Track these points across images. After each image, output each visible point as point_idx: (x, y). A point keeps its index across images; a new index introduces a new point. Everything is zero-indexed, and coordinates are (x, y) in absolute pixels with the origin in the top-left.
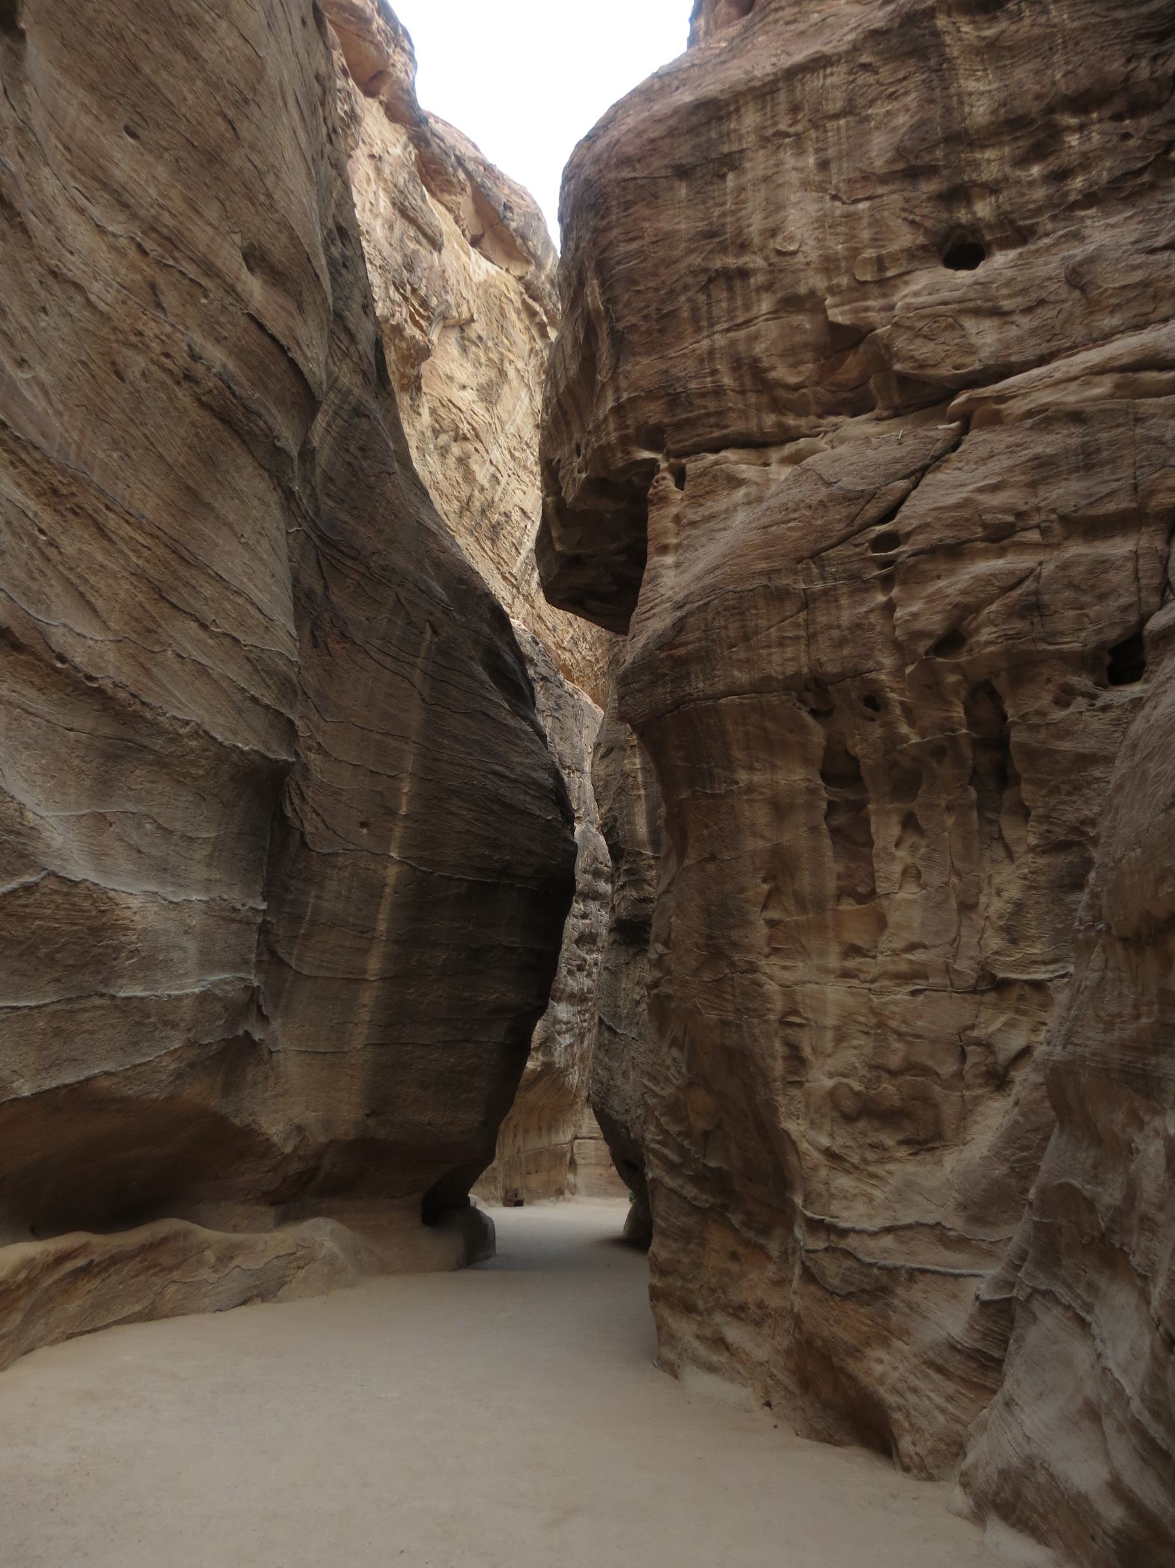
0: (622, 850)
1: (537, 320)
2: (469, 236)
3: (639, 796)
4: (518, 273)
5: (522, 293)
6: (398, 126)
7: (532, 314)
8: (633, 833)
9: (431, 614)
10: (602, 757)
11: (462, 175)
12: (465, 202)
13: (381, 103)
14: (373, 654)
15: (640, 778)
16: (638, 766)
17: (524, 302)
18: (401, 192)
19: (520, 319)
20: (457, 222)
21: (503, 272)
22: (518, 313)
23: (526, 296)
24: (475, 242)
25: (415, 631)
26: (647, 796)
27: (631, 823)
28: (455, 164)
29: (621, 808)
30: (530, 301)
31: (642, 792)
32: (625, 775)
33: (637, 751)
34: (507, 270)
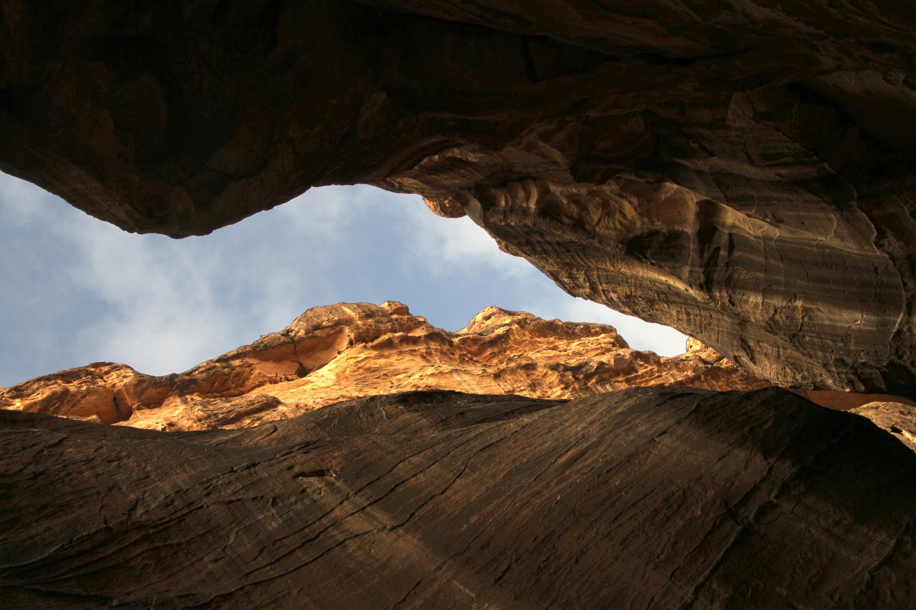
0: (891, 365)
1: (397, 341)
2: (295, 376)
3: (806, 311)
4: (346, 343)
5: (365, 347)
6: (166, 402)
7: (389, 344)
8: (862, 336)
9: (291, 468)
10: (752, 359)
11: (237, 362)
12: (261, 368)
13: (139, 409)
14: (272, 574)
15: (778, 302)
16: (760, 299)
17: (374, 348)
18: (209, 417)
19: (387, 357)
20: (276, 382)
21: (339, 357)
22: (381, 356)
23: (370, 344)
24: (303, 372)
25: (293, 499)
26: (807, 298)
27: (845, 336)
28: (224, 364)
29: (823, 348)
30: (376, 342)
31: (799, 303)
32: (772, 327)
33: (738, 296)
34: (339, 353)
